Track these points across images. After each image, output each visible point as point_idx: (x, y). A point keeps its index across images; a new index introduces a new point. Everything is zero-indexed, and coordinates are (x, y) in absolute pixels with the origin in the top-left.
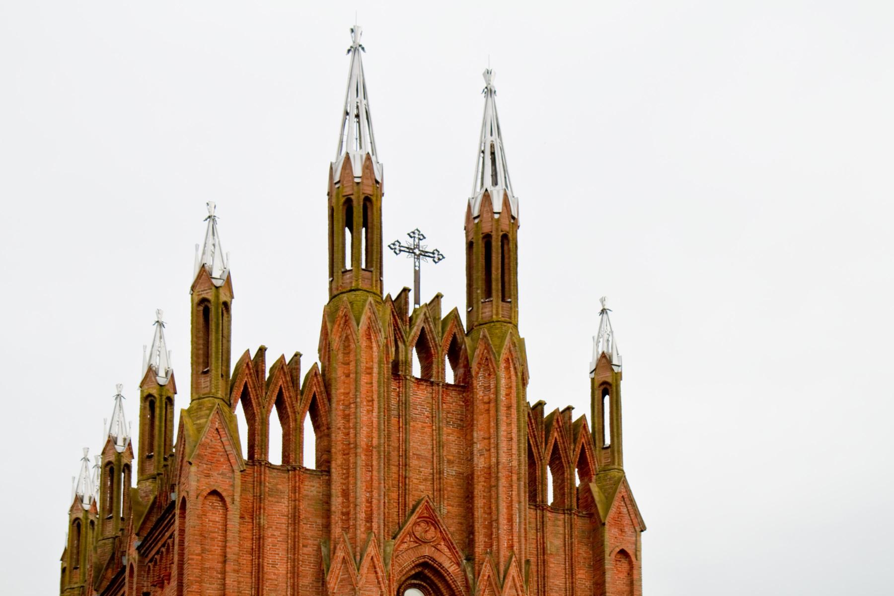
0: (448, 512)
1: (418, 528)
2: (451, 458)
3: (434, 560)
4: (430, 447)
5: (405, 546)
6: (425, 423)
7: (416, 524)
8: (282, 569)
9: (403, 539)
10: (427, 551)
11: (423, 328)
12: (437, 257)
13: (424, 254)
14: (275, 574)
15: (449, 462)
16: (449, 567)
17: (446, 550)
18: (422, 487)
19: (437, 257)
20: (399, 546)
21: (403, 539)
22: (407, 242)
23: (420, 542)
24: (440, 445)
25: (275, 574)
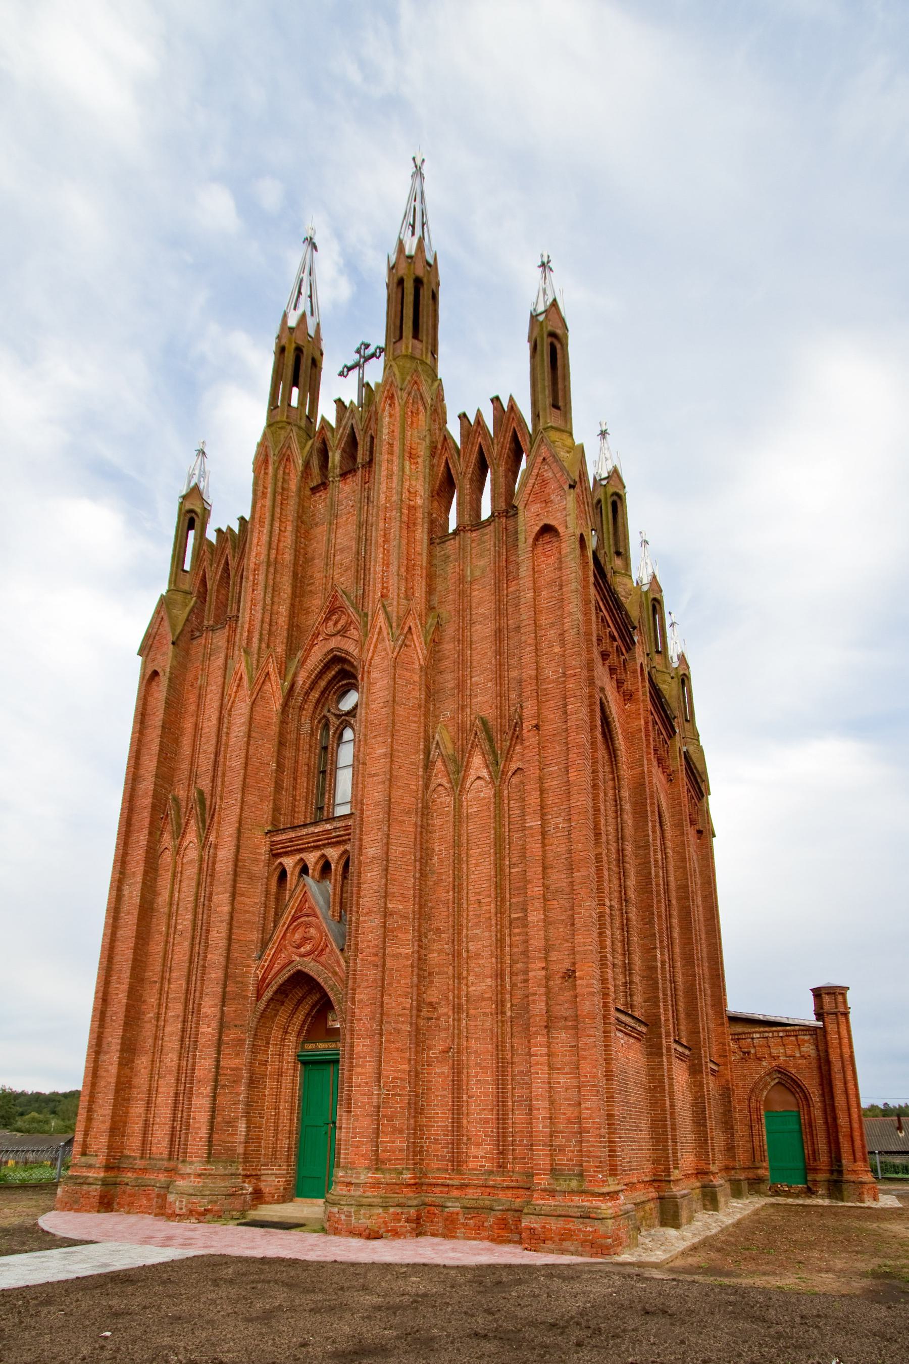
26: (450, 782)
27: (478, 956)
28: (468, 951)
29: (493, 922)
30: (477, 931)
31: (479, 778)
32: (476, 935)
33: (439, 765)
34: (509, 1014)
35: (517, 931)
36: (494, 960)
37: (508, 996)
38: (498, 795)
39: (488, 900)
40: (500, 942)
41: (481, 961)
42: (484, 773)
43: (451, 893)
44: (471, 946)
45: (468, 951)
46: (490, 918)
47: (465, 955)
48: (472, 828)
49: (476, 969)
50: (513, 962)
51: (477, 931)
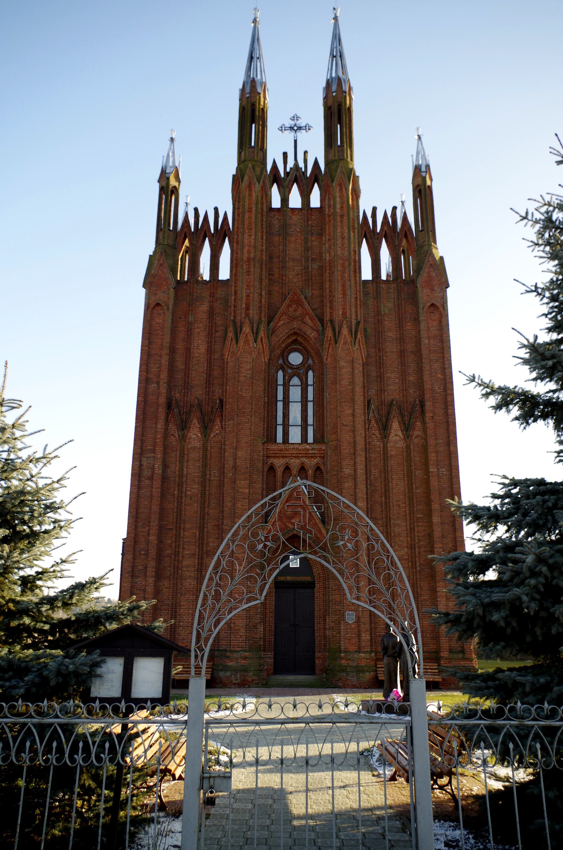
0: (312, 295)
1: (291, 309)
2: (314, 256)
3: (301, 330)
4: (300, 252)
5: (282, 322)
6: (297, 236)
7: (289, 306)
8: (203, 349)
9: (280, 318)
10: (295, 325)
11: (296, 175)
12: (307, 128)
13: (300, 128)
14: (198, 353)
15: (313, 260)
16: (311, 334)
17: (310, 321)
18: (295, 280)
19: (307, 128)
20: (277, 323)
21: (280, 318)
22: (288, 123)
23: (293, 319)
24: (307, 249)
25: (198, 353)
26: (380, 434)
27: (399, 535)
28: (394, 532)
29: (408, 518)
30: (399, 522)
31: (396, 435)
32: (398, 524)
33: (373, 422)
34: (418, 569)
35: (420, 524)
36: (409, 539)
37: (417, 559)
38: (408, 447)
39: (404, 505)
40: (412, 530)
41: (401, 539)
42: (400, 433)
43: (383, 499)
44: (396, 530)
45: (394, 532)
46: (406, 515)
47: (393, 534)
48: (392, 462)
49: (399, 543)
50: (419, 541)
51: (399, 522)
